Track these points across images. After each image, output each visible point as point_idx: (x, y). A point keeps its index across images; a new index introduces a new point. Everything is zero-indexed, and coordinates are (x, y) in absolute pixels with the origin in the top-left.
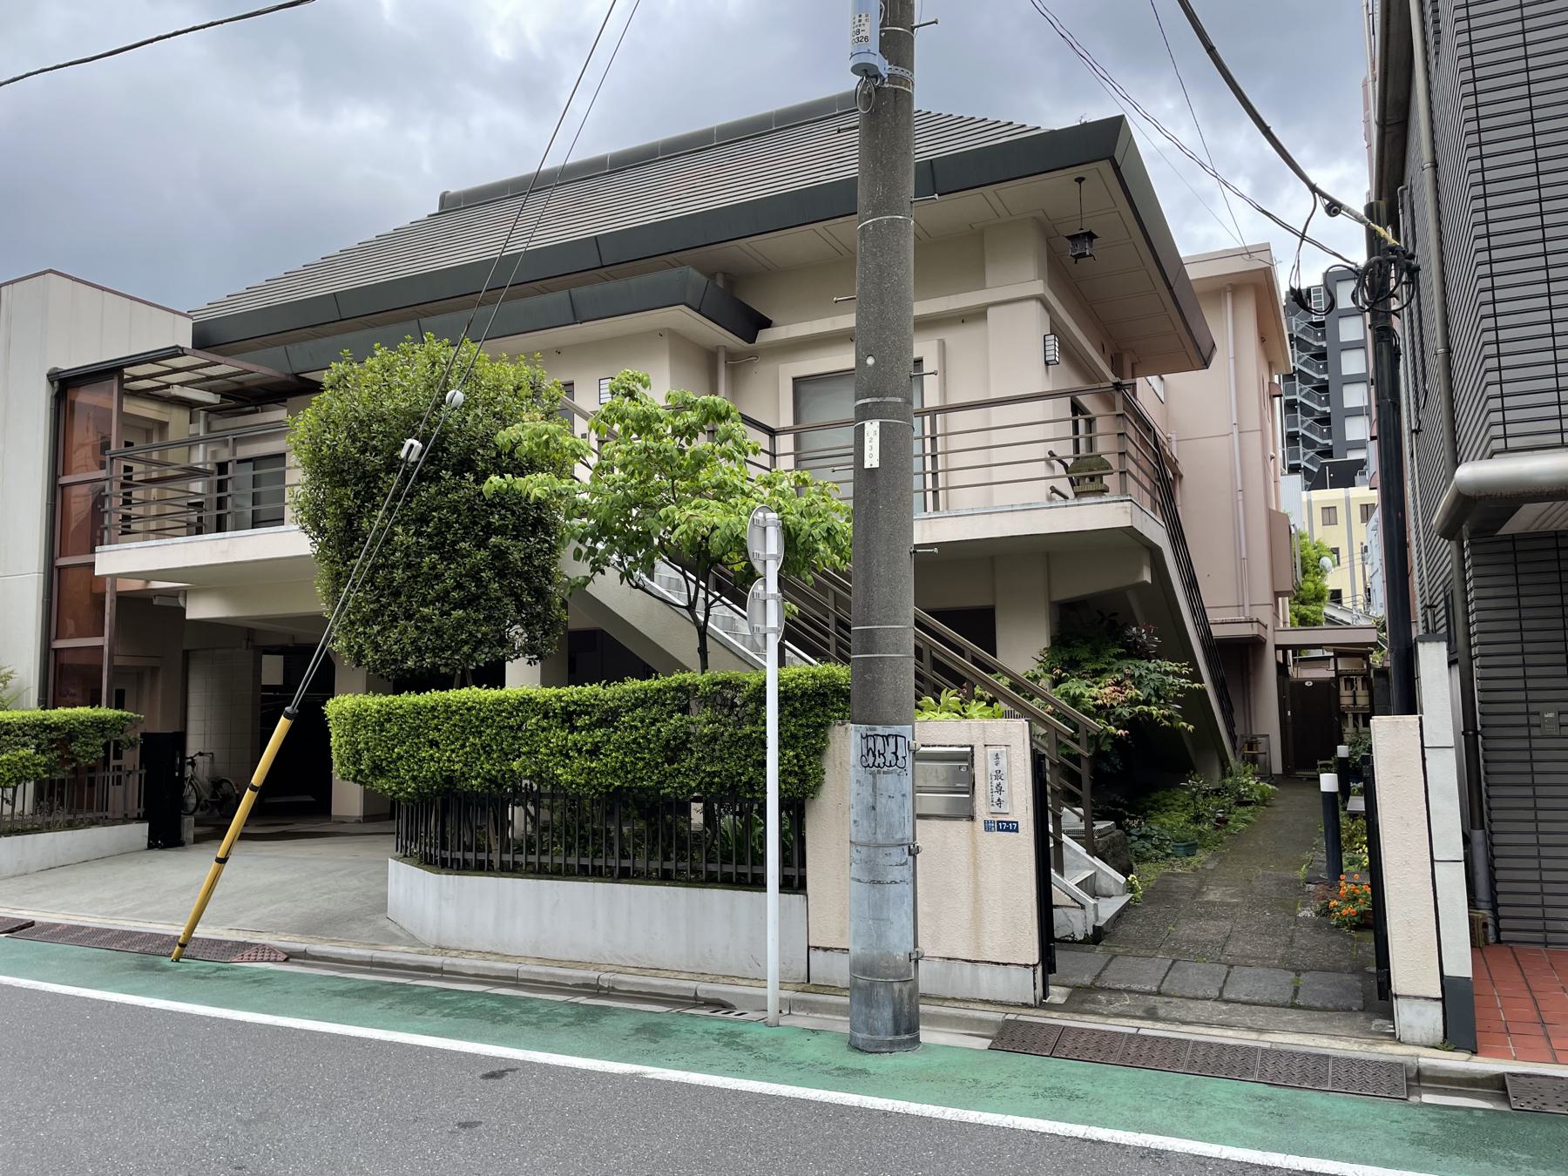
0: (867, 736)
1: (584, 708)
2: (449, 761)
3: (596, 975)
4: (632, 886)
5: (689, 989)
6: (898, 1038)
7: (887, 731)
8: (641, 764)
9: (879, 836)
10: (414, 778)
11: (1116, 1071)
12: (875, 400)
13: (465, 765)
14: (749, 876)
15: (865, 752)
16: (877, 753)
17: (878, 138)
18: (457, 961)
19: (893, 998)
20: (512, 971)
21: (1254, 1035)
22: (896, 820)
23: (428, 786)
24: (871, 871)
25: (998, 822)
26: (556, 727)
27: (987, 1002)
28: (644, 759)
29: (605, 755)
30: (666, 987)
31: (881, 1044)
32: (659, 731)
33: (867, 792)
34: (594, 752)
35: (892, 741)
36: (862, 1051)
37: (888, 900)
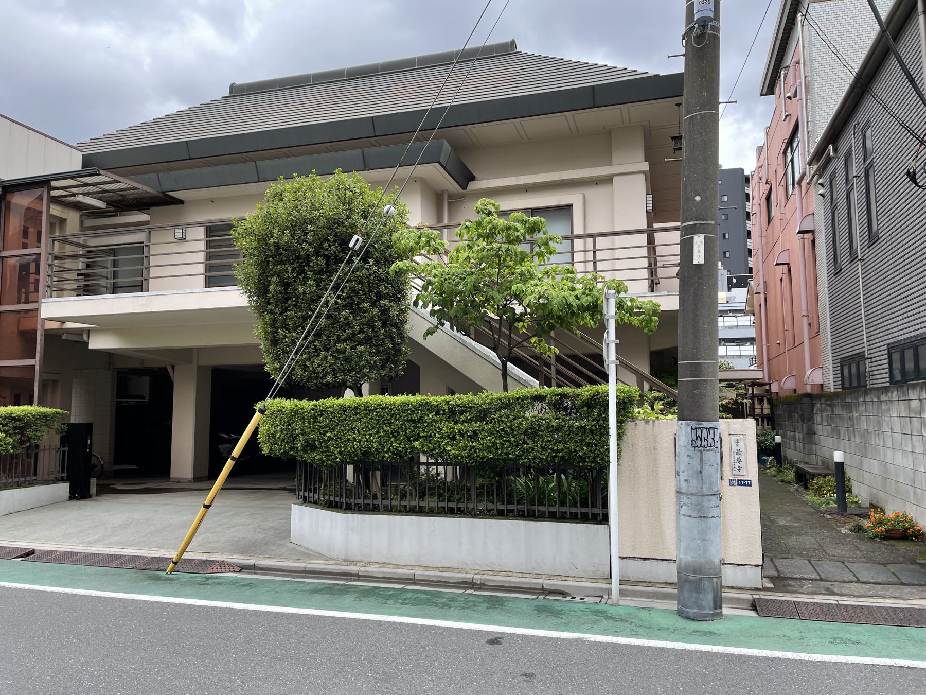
0: (696, 428)
1: (464, 409)
2: (367, 441)
3: (471, 576)
4: (487, 520)
5: (538, 584)
6: (716, 611)
7: (709, 425)
8: (507, 444)
9: (705, 489)
10: (340, 453)
11: (825, 625)
12: (702, 222)
13: (380, 444)
14: (568, 513)
15: (694, 438)
16: (703, 439)
17: (704, 63)
18: (367, 569)
19: (713, 587)
20: (411, 574)
21: (902, 602)
22: (714, 479)
23: (351, 457)
24: (699, 511)
25: (738, 480)
26: (445, 421)
27: (732, 588)
28: (509, 441)
29: (482, 439)
30: (522, 583)
31: (707, 615)
32: (521, 424)
33: (696, 463)
34: (475, 435)
35: (711, 431)
36: (694, 620)
37: (710, 528)
